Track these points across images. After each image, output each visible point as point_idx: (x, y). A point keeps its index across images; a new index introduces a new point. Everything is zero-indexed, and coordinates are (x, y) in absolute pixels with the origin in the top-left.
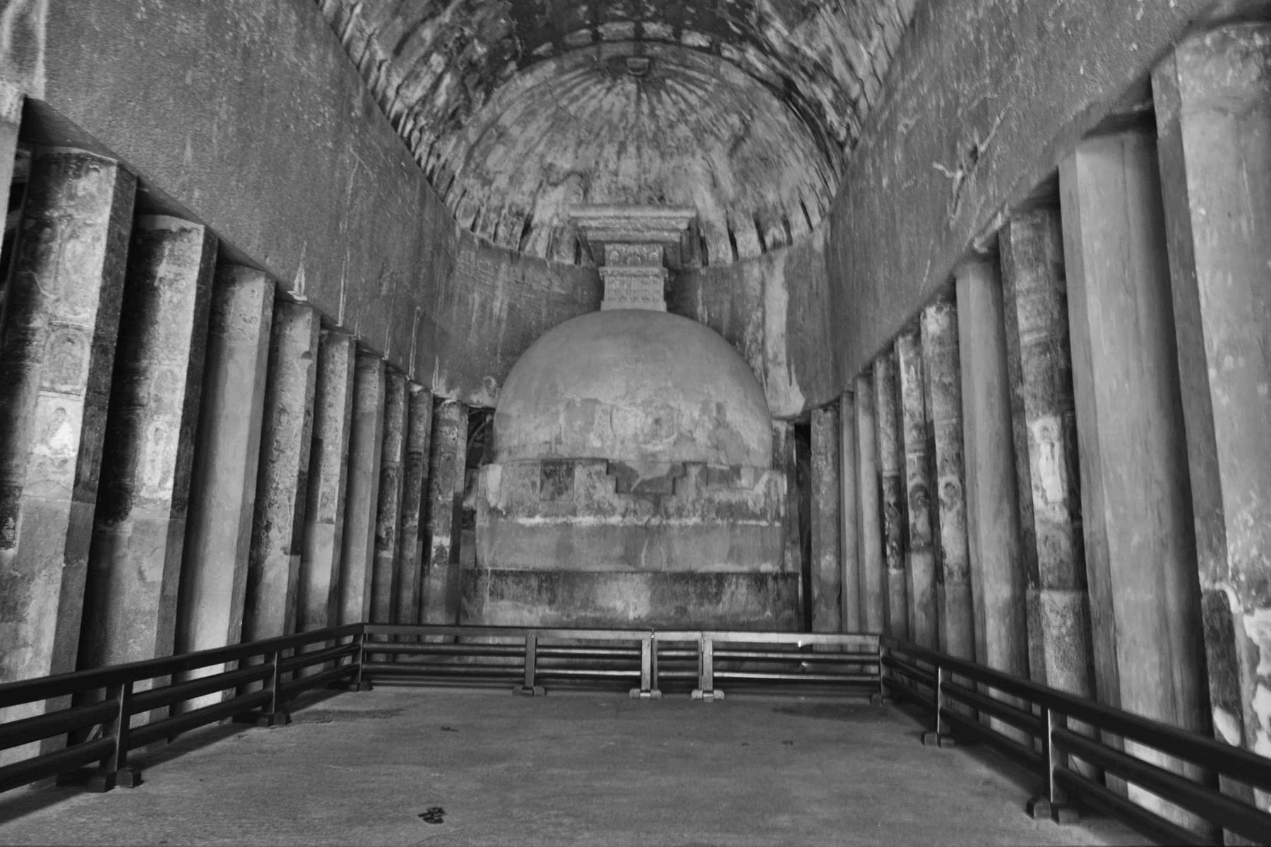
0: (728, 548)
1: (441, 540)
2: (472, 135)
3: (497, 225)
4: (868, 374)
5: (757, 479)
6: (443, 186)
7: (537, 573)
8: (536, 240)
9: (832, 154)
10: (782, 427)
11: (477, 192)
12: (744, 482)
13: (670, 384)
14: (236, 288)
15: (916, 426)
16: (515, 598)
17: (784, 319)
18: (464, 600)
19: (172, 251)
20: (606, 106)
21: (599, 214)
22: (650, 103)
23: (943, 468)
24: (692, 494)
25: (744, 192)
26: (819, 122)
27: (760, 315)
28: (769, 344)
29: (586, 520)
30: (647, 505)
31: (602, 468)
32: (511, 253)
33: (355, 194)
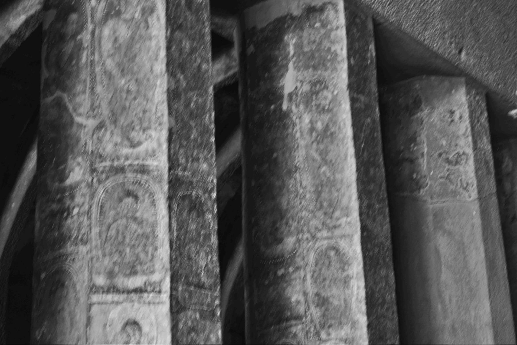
14: (424, 113)
19: (299, 46)
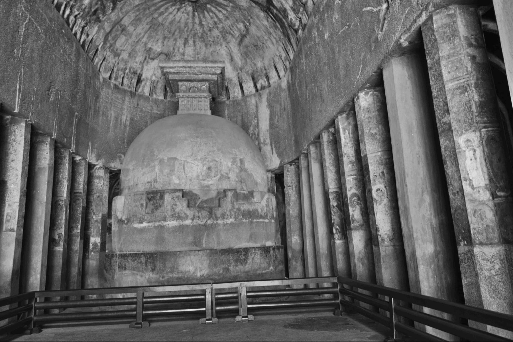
0: (249, 235)
1: (95, 239)
2: (107, 27)
3: (123, 78)
4: (317, 141)
5: (262, 198)
6: (91, 53)
7: (144, 254)
8: (144, 87)
9: (291, 37)
10: (270, 175)
11: (111, 60)
12: (255, 200)
13: (215, 149)
15: (351, 162)
16: (133, 269)
17: (268, 122)
18: (105, 271)
20: (177, 19)
21: (175, 65)
22: (199, 18)
23: (374, 181)
24: (229, 207)
25: (247, 63)
26: (284, 20)
27: (256, 121)
28: (261, 135)
29: (172, 223)
30: (205, 213)
31: (180, 194)
32: (131, 92)
33: (27, 35)
